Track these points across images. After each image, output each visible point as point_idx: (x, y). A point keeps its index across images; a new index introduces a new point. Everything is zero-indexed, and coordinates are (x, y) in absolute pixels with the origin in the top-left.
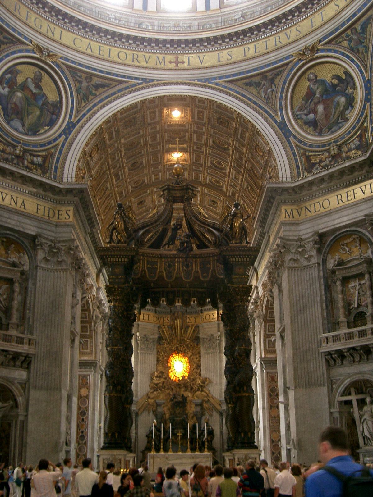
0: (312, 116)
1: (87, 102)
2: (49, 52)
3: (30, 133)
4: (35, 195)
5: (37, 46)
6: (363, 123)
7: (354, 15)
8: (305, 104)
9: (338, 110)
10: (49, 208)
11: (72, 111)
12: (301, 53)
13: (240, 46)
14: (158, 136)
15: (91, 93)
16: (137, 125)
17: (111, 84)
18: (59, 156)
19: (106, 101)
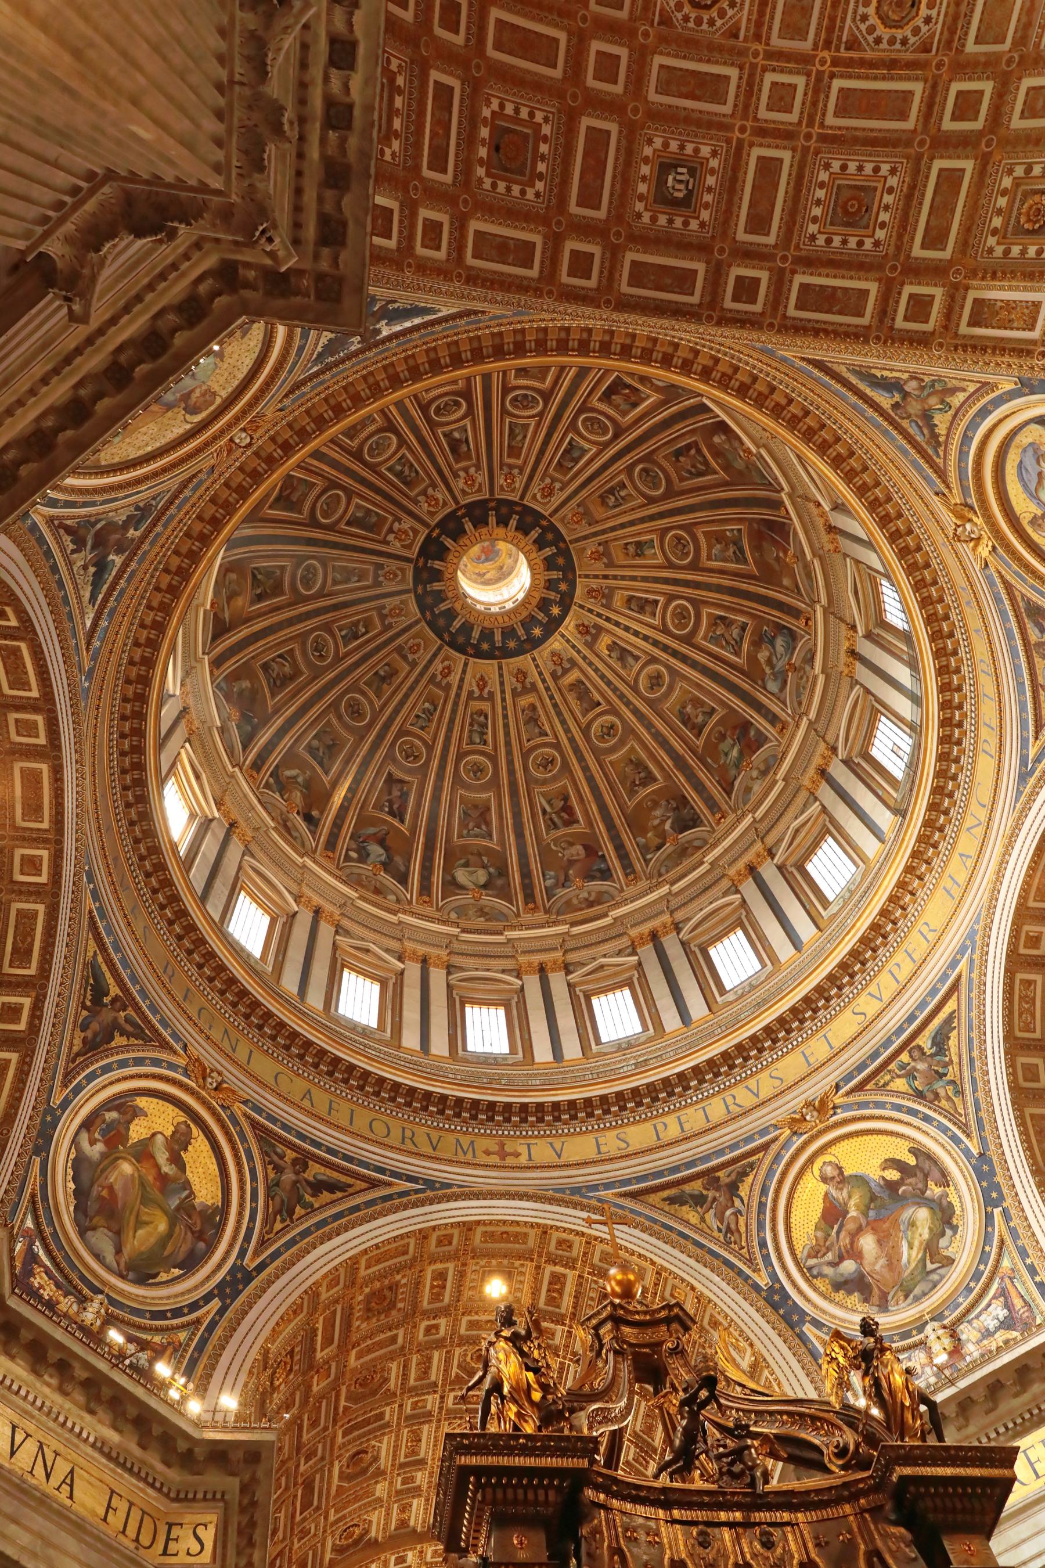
0: (849, 1266)
1: (288, 1222)
2: (223, 1081)
3: (131, 1275)
4: (114, 1454)
5: (198, 1060)
6: (998, 1261)
7: (911, 1018)
8: (826, 1240)
9: (916, 1243)
10: (144, 1512)
11: (247, 1238)
12: (797, 1116)
13: (645, 1120)
14: (436, 1355)
15: (300, 1200)
16: (394, 1312)
17: (350, 1186)
18: (196, 1355)
19: (335, 1224)
